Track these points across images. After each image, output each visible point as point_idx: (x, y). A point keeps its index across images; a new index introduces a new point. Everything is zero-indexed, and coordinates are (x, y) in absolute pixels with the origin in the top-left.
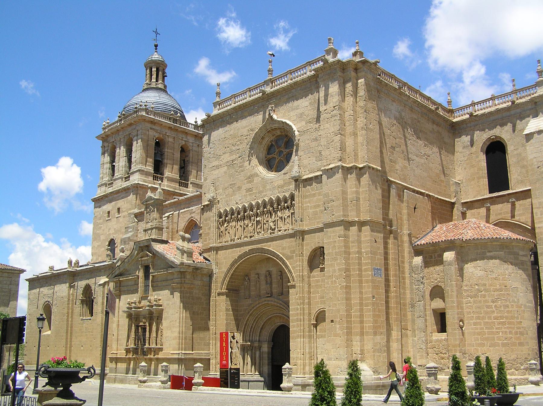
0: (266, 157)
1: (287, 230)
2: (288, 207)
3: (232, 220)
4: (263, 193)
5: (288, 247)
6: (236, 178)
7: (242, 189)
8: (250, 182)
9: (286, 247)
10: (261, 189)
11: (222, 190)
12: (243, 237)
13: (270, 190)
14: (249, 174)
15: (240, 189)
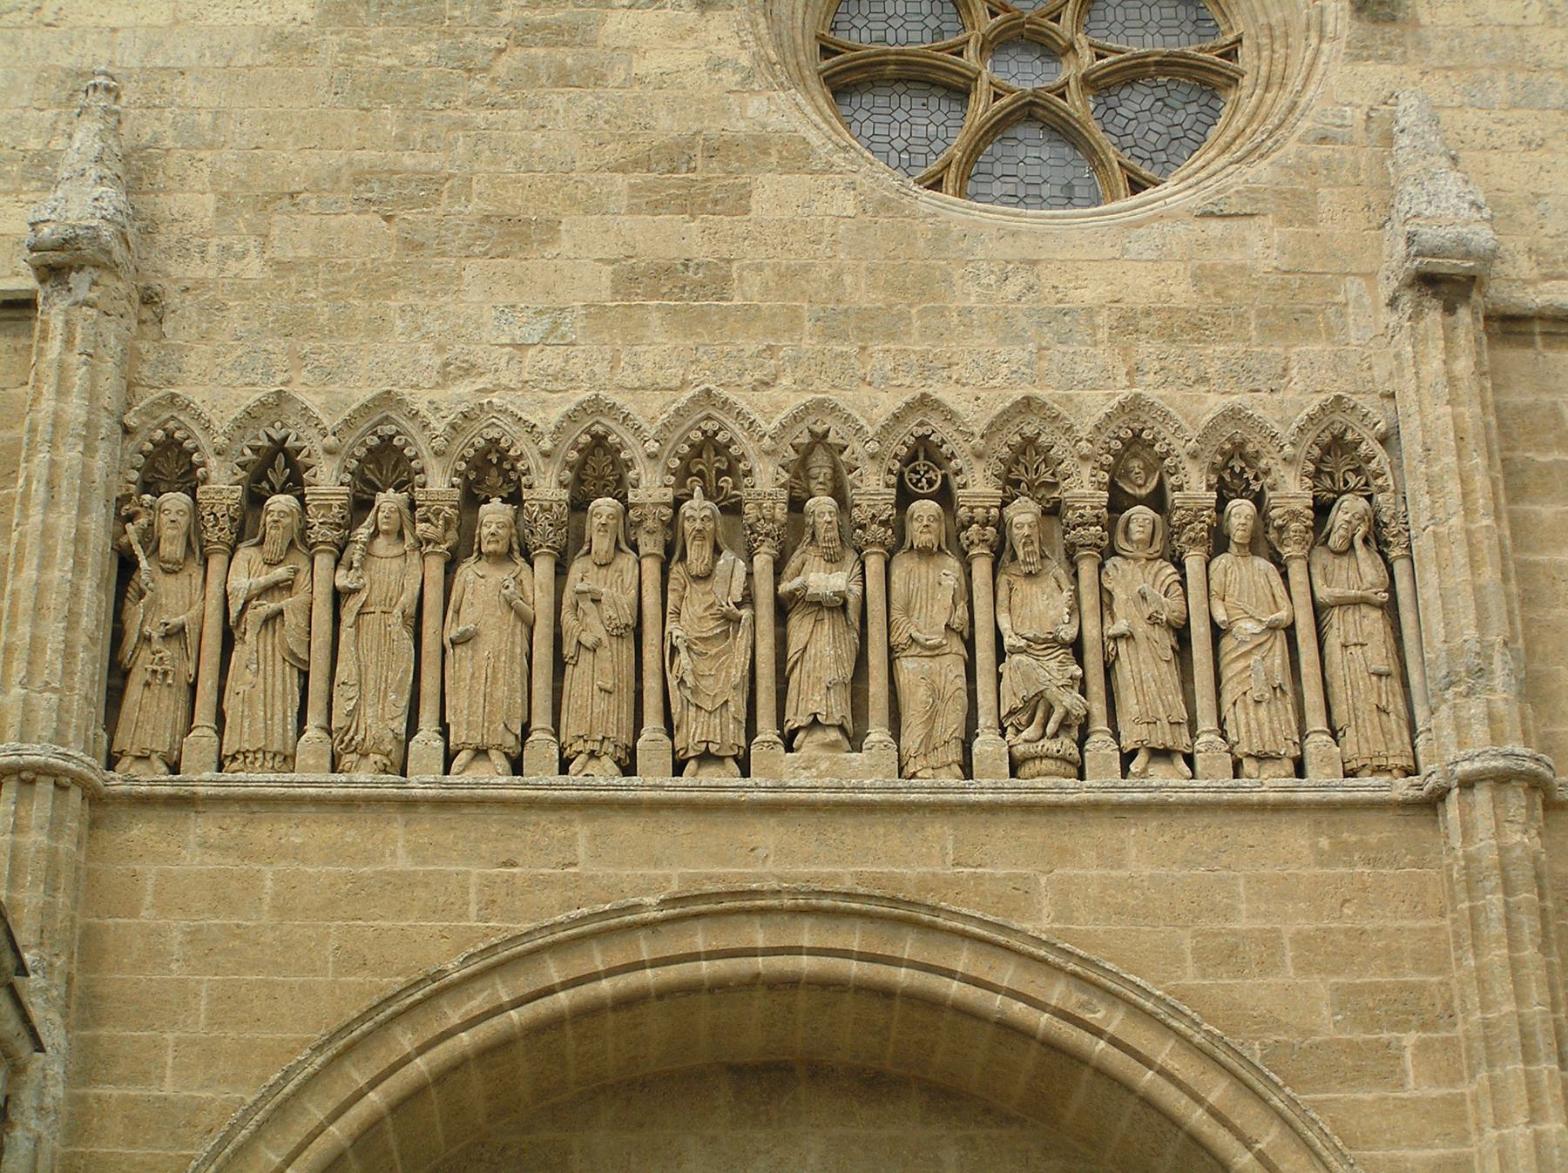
0: (826, 51)
1: (1279, 758)
2: (1264, 543)
3: (363, 532)
4: (892, 336)
5: (1301, 940)
6: (464, 125)
7: (565, 245)
8: (689, 203)
9: (1270, 941)
10: (863, 295)
11: (210, 200)
12: (542, 748)
13: (1004, 326)
14: (667, 126)
15: (526, 239)
